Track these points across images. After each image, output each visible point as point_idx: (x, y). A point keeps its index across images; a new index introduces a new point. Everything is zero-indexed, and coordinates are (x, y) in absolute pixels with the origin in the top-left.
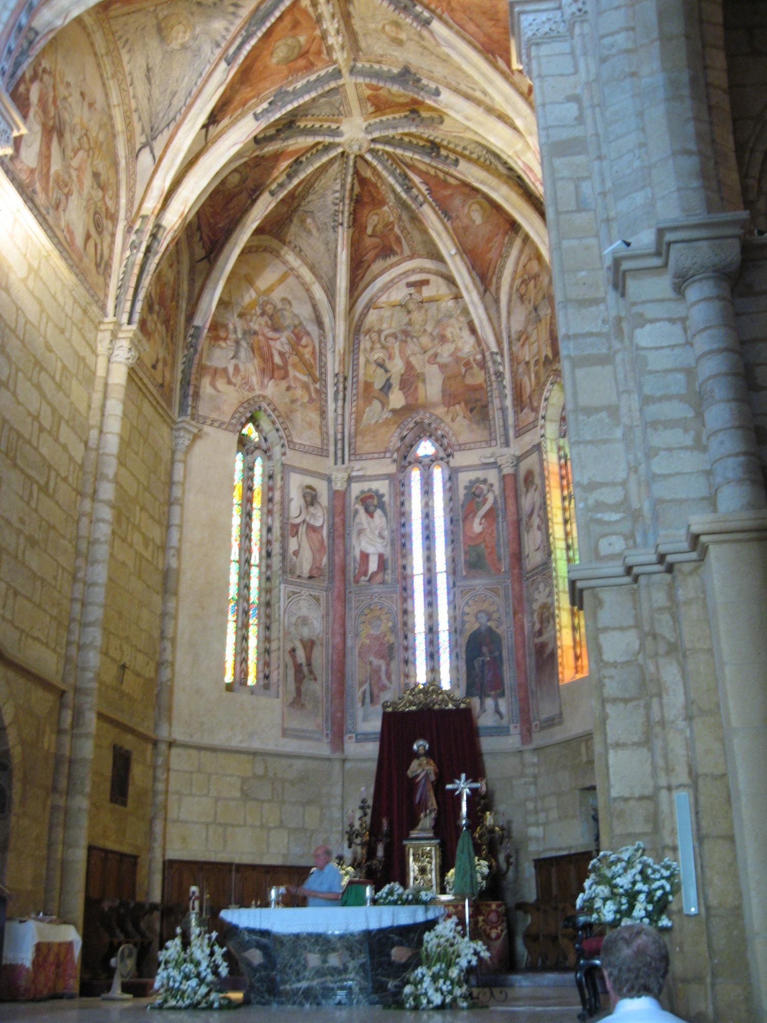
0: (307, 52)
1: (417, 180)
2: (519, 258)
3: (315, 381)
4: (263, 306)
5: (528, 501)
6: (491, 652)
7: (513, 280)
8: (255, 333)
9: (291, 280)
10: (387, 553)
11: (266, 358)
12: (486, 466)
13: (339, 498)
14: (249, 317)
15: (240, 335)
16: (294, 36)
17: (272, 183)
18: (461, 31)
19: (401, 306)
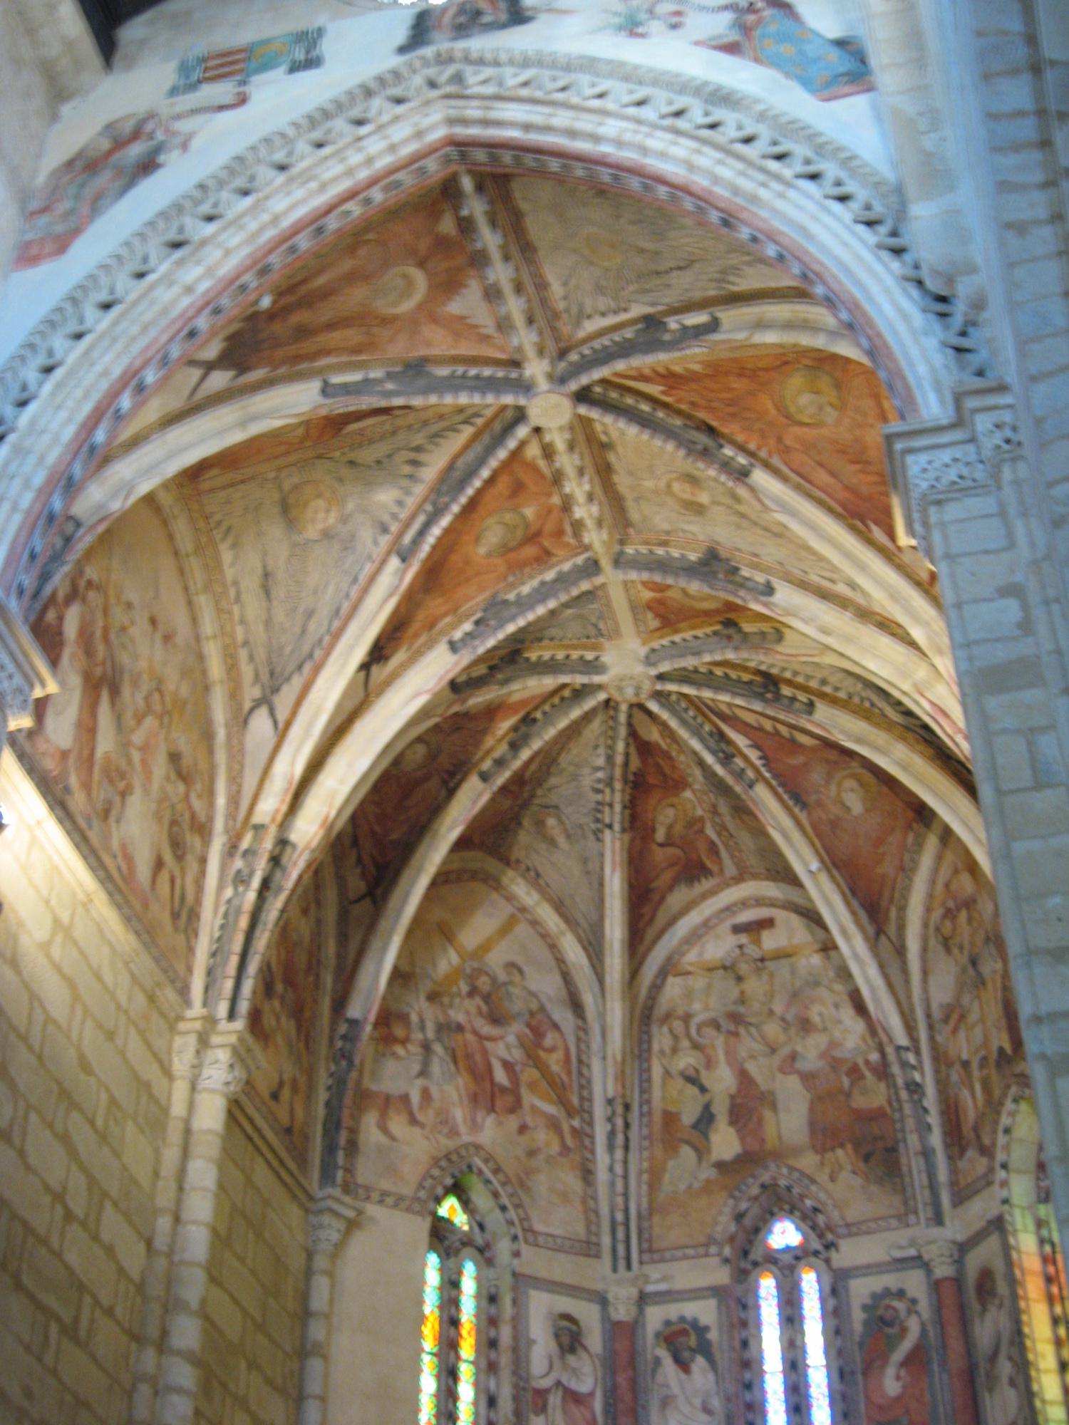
0: (538, 534)
1: (741, 741)
2: (936, 870)
3: (570, 1113)
4: (472, 979)
5: (986, 1330)
7: (928, 910)
8: (460, 1028)
9: (522, 929)
11: (480, 1074)
12: (901, 1264)
13: (623, 1335)
14: (446, 1000)
15: (430, 1033)
16: (515, 509)
17: (482, 759)
18: (804, 484)
19: (725, 968)
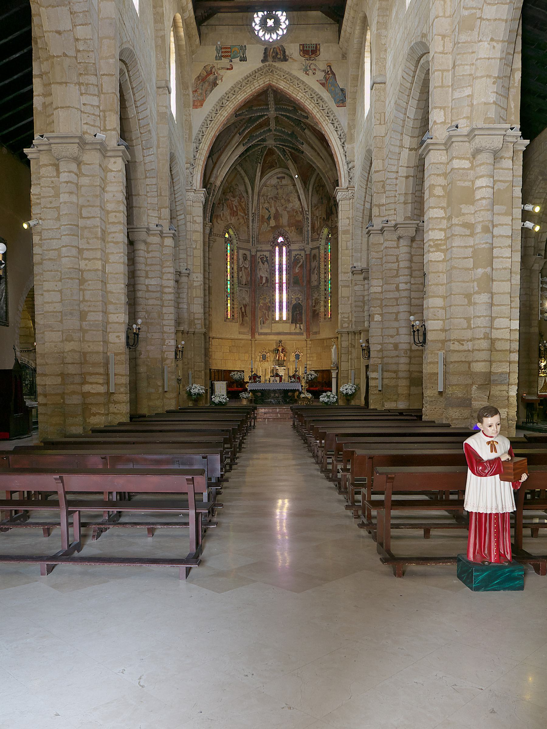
6: (299, 310)
7: (315, 183)
10: (269, 277)
11: (232, 209)
12: (301, 250)
